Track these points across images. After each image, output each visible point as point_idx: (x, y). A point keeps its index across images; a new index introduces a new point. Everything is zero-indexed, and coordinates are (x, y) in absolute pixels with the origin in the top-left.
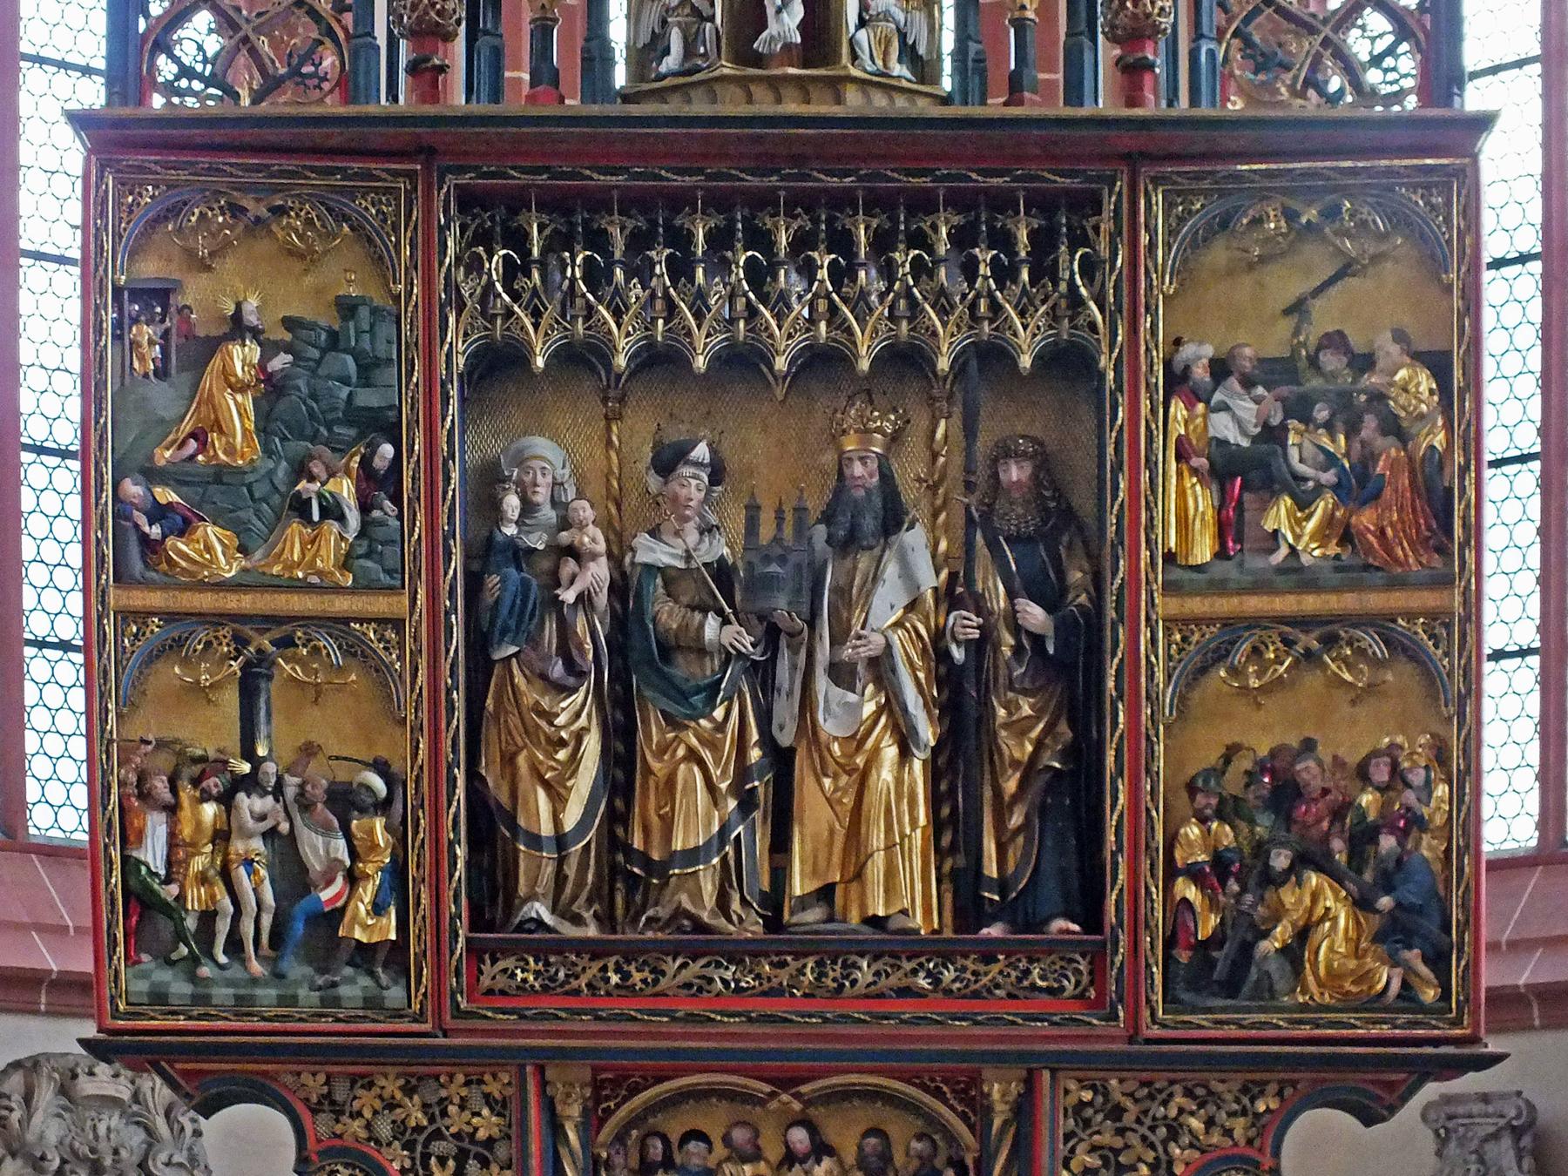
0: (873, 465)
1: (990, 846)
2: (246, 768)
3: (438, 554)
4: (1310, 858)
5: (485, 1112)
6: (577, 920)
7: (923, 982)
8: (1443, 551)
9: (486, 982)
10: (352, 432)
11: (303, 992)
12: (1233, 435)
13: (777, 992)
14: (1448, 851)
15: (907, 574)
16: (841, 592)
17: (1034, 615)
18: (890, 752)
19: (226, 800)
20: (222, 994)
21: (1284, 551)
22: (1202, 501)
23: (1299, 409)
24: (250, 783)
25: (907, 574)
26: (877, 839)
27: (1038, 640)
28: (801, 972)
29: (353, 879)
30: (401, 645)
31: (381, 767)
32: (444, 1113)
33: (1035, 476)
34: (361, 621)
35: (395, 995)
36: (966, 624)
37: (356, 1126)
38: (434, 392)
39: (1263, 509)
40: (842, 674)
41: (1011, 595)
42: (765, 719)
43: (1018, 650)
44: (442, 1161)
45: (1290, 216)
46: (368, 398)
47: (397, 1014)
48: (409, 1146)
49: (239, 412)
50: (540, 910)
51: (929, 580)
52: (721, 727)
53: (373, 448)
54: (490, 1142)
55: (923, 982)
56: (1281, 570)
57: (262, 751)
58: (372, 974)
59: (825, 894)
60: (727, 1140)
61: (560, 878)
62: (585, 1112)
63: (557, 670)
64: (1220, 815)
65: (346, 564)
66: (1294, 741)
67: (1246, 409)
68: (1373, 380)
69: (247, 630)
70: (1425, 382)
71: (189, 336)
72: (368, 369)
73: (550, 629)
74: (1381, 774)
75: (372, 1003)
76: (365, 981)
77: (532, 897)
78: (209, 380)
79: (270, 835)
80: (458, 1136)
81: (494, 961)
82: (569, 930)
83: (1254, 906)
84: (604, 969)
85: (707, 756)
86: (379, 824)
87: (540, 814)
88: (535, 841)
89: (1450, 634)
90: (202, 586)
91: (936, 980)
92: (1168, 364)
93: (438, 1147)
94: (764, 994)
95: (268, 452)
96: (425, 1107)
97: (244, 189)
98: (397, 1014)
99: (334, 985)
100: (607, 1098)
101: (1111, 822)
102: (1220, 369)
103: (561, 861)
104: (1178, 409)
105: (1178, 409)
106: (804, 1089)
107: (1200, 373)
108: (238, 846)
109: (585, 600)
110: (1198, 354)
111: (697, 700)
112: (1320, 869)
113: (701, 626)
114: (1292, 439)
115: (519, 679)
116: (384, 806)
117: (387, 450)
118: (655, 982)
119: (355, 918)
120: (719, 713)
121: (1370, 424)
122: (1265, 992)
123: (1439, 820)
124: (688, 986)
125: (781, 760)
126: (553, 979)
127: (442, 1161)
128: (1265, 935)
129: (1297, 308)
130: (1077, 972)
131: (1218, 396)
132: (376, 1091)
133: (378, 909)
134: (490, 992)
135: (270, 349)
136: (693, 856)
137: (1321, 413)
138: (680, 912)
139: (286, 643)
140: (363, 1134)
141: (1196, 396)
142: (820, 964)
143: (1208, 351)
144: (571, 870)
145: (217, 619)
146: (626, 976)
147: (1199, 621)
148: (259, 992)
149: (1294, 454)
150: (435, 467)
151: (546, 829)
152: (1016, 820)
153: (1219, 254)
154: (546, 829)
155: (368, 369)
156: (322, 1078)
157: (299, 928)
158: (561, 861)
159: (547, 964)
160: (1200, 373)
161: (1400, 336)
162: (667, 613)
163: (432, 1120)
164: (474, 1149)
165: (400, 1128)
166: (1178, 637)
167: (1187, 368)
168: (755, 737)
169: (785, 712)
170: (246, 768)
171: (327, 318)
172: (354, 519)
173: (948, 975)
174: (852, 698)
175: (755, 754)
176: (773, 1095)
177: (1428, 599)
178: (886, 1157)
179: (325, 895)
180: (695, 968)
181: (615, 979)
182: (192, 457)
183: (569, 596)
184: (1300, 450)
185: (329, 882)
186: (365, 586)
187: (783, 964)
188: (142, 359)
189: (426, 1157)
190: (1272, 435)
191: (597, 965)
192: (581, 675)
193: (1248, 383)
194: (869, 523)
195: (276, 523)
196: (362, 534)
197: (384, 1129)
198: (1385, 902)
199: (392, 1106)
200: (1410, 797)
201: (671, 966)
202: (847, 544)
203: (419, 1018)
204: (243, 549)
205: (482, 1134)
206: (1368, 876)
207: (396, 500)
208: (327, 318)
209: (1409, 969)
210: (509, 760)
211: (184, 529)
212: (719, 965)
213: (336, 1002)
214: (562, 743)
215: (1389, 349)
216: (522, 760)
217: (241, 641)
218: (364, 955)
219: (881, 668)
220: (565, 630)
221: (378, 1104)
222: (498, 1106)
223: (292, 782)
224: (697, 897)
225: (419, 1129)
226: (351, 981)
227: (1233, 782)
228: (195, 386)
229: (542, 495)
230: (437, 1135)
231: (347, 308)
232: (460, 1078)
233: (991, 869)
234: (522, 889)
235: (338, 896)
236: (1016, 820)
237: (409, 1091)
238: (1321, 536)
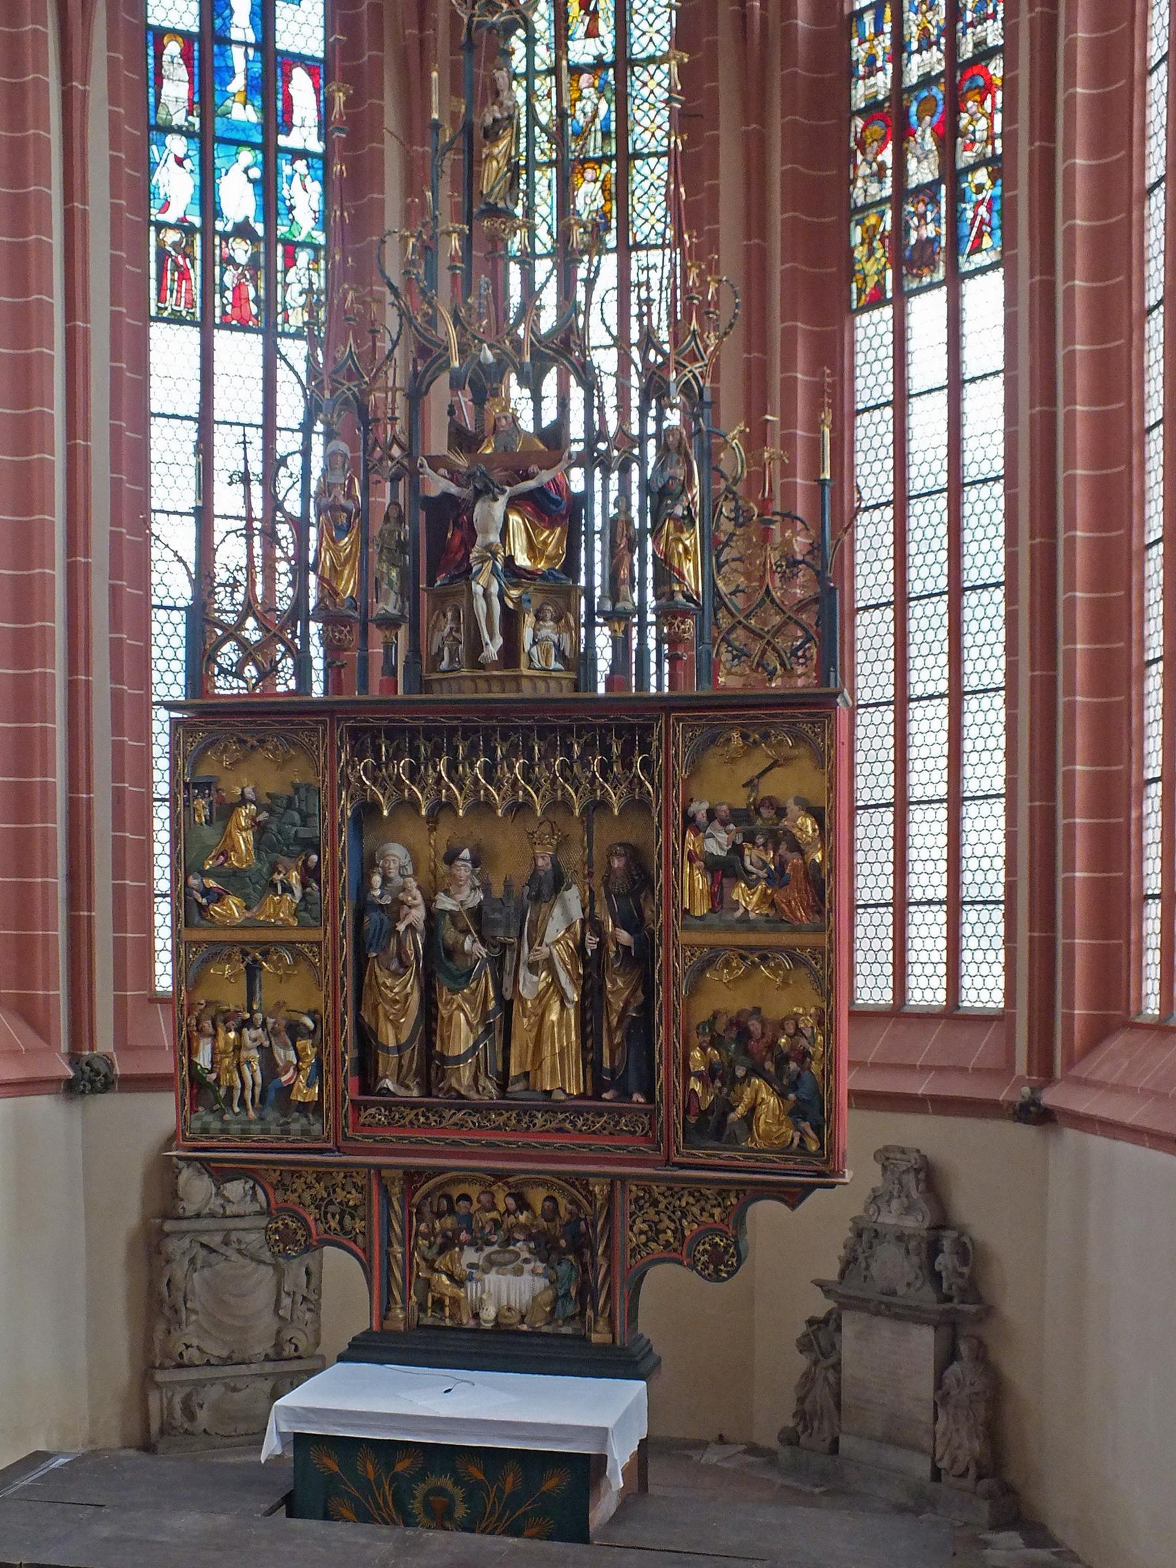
0: (548, 860)
1: (606, 1052)
2: (248, 1016)
3: (337, 908)
4: (756, 1071)
5: (353, 1191)
6: (407, 1087)
7: (568, 1126)
8: (820, 912)
9: (362, 1120)
10: (298, 848)
11: (273, 1127)
12: (717, 851)
13: (498, 1128)
14: (823, 1071)
15: (566, 912)
16: (534, 924)
17: (624, 936)
18: (556, 1006)
19: (239, 1031)
20: (235, 1127)
21: (741, 910)
22: (701, 882)
23: (750, 838)
24: (248, 1023)
25: (566, 912)
26: (546, 1051)
27: (627, 949)
28: (509, 1119)
29: (298, 1069)
30: (320, 953)
31: (311, 1014)
32: (334, 1192)
33: (627, 865)
34: (301, 943)
35: (316, 1128)
36: (592, 942)
37: (293, 1197)
38: (336, 830)
39: (733, 886)
40: (533, 968)
41: (615, 926)
42: (498, 986)
43: (617, 952)
44: (333, 1216)
45: (744, 737)
46: (304, 833)
47: (316, 1139)
48: (318, 1207)
49: (244, 840)
50: (389, 1084)
51: (577, 914)
52: (474, 992)
53: (307, 856)
54: (355, 1207)
55: (568, 1126)
56: (739, 921)
57: (255, 1007)
58: (307, 1117)
59: (526, 1075)
60: (479, 1201)
61: (400, 1066)
62: (402, 1192)
63: (394, 966)
64: (712, 1044)
65: (295, 914)
66: (748, 1007)
67: (723, 837)
68: (785, 823)
69: (248, 948)
70: (809, 823)
71: (221, 801)
72: (305, 818)
73: (393, 942)
74: (791, 1029)
75: (305, 1132)
76: (304, 1121)
77: (386, 1077)
78: (232, 825)
79: (260, 1048)
80: (340, 1203)
81: (366, 1110)
82: (402, 1092)
83: (728, 1094)
84: (417, 1115)
85: (467, 1007)
86: (308, 1043)
87: (389, 1036)
88: (387, 1049)
89: (823, 959)
90: (226, 927)
91: (575, 1126)
92: (685, 812)
93: (331, 1209)
94: (494, 1129)
95: (259, 859)
96: (326, 1188)
97: (245, 732)
98: (316, 1139)
99: (288, 1123)
100: (416, 1182)
101: (657, 1048)
102: (711, 814)
103: (401, 1058)
104: (690, 836)
105: (690, 836)
106: (509, 1180)
107: (702, 817)
108: (244, 1054)
109: (410, 927)
110: (699, 808)
111: (462, 980)
112: (759, 1076)
113: (464, 941)
114: (747, 852)
115: (377, 970)
116: (311, 1034)
117: (314, 858)
118: (441, 1122)
119: (299, 1089)
120: (473, 985)
121: (783, 848)
122: (733, 1140)
123: (818, 1055)
124: (456, 1124)
125: (506, 1007)
126: (393, 1119)
127: (333, 1216)
128: (733, 1109)
129: (750, 784)
130: (643, 1123)
131: (709, 831)
132: (303, 1179)
133: (309, 1085)
134: (364, 1125)
135: (261, 808)
136: (459, 1059)
137: (760, 840)
138: (451, 1088)
139: (265, 954)
140: (298, 1201)
141: (697, 831)
142: (518, 1115)
143: (706, 806)
144: (405, 1062)
145: (233, 944)
146: (427, 1118)
147: (700, 946)
148: (252, 1127)
149: (747, 860)
150: (336, 868)
151: (392, 1043)
152: (617, 1040)
153: (713, 760)
154: (392, 1043)
155: (305, 818)
156: (278, 1173)
157: (272, 1095)
158: (401, 1058)
159: (390, 1111)
160: (702, 817)
161: (799, 801)
162: (449, 934)
163: (329, 1195)
164: (348, 1210)
165: (314, 1198)
166: (688, 953)
167: (694, 815)
168: (492, 994)
169: (508, 982)
170: (248, 1016)
171: (290, 792)
172: (298, 892)
173: (580, 1123)
174: (535, 978)
175: (492, 1005)
176: (494, 1183)
177: (810, 939)
178: (556, 1210)
179: (284, 1079)
180: (460, 1115)
181: (422, 1119)
182: (222, 864)
183: (401, 927)
184: (751, 856)
185: (287, 1072)
186: (302, 926)
187: (501, 1114)
188: (199, 816)
189: (326, 1213)
190: (737, 850)
191: (415, 1112)
192: (407, 967)
193: (724, 823)
194: (545, 890)
195: (262, 894)
196: (303, 899)
197: (307, 1198)
198: (792, 1096)
199: (310, 1187)
200: (804, 1042)
201: (447, 1114)
202: (537, 898)
203: (327, 1140)
204: (248, 908)
205: (351, 1203)
206: (785, 1082)
207: (318, 883)
208: (290, 792)
209: (803, 1133)
210: (375, 1007)
211: (219, 897)
212: (470, 1114)
213: (288, 1132)
214: (397, 1002)
215: (792, 808)
216: (380, 1007)
217: (245, 954)
218: (303, 1107)
219: (549, 964)
220: (400, 944)
221: (304, 1187)
222: (360, 1189)
223: (270, 1021)
224: (459, 1080)
225: (322, 1199)
226: (296, 1120)
227: (721, 1026)
228: (225, 828)
229: (393, 873)
230: (331, 1202)
231: (297, 788)
232: (342, 1174)
233: (607, 1064)
234: (380, 1074)
235: (290, 1079)
236: (617, 1040)
237: (318, 1180)
238: (758, 905)
